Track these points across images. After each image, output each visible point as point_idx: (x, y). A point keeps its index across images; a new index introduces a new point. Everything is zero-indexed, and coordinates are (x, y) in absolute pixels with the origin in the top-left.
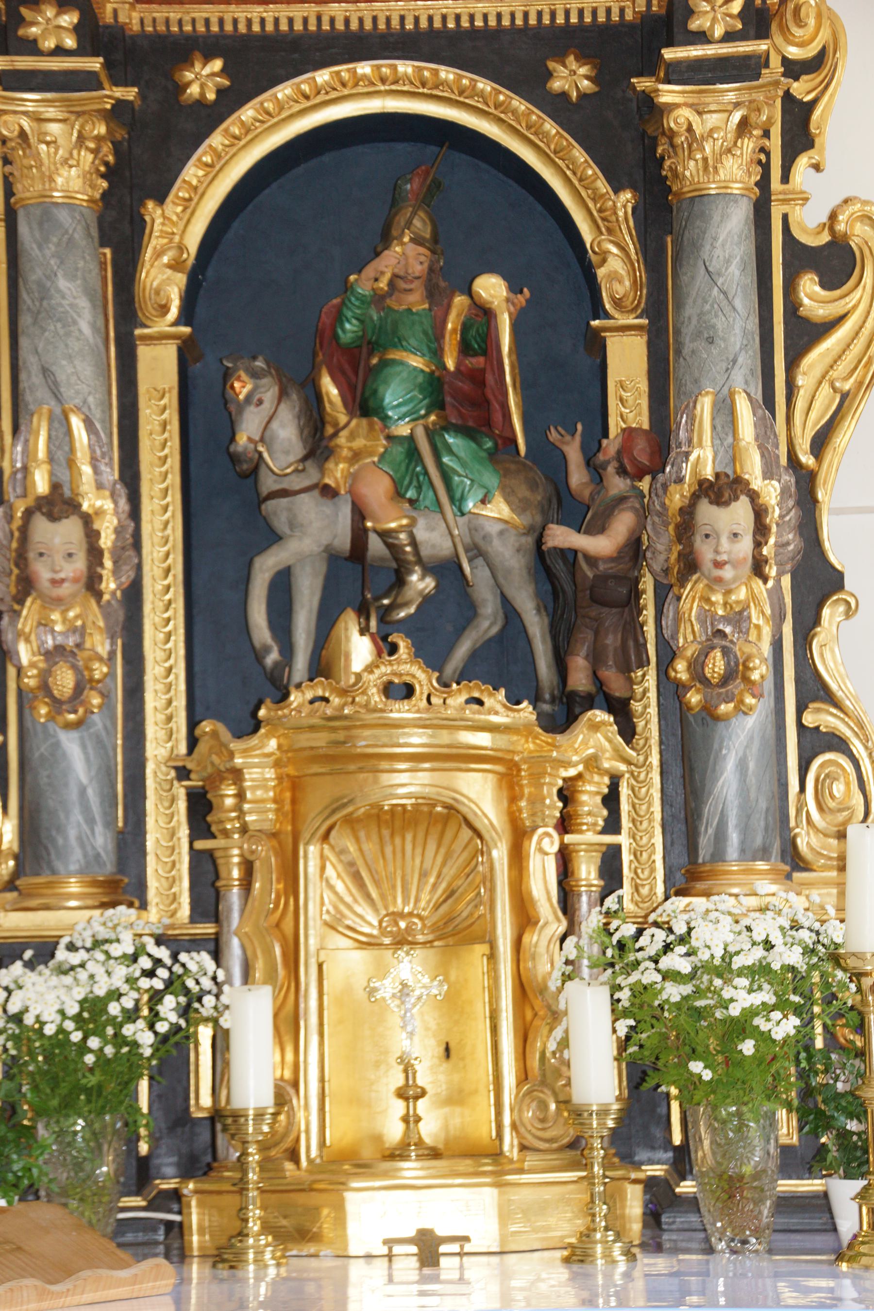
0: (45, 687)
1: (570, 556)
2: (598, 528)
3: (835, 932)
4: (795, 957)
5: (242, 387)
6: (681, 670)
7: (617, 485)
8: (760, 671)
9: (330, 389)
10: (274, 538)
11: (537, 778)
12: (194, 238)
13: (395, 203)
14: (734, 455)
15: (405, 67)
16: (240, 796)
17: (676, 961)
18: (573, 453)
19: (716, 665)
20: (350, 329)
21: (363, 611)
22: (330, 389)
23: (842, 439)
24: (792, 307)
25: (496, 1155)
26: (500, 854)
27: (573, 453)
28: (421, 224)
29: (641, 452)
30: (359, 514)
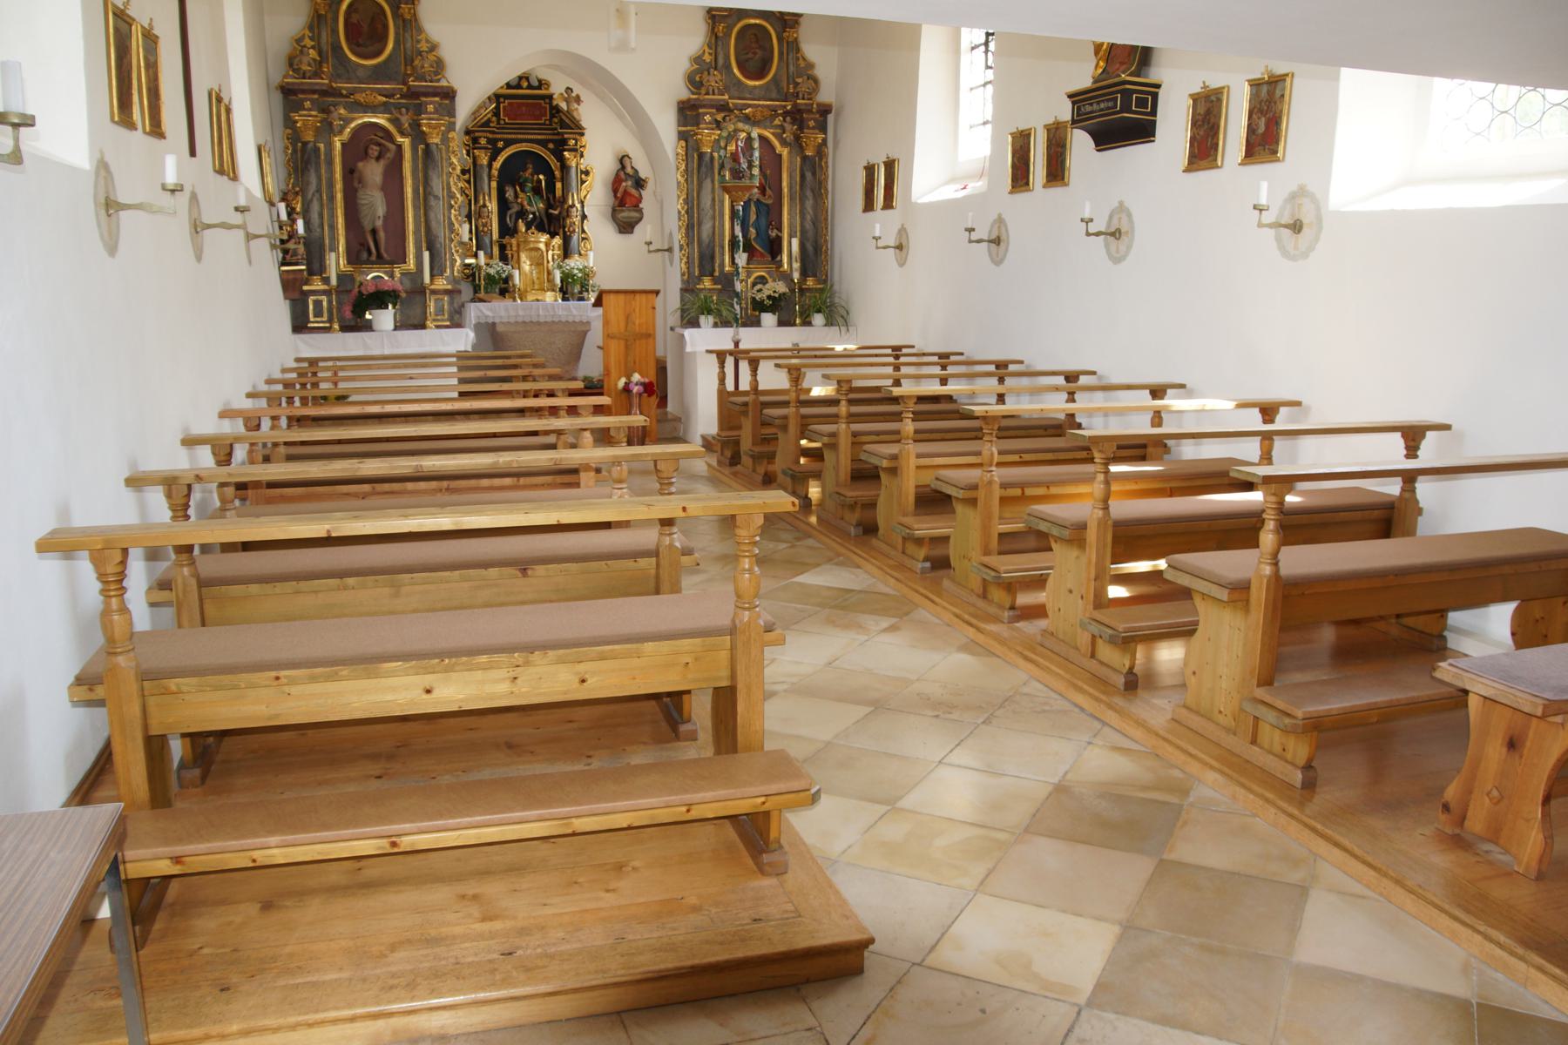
0: (483, 231)
1: (551, 214)
2: (555, 210)
3: (586, 264)
4: (581, 267)
5: (507, 188)
6: (566, 229)
7: (558, 204)
8: (577, 230)
9: (517, 187)
10: (509, 209)
11: (550, 244)
12: (498, 166)
13: (526, 164)
14: (573, 201)
15: (529, 144)
16: (511, 246)
17: (568, 267)
18: (551, 198)
19: (571, 229)
20: (521, 181)
21: (522, 219)
22: (517, 187)
23: (588, 197)
24: (581, 179)
25: (544, 290)
26: (545, 254)
27: (551, 198)
28: (531, 166)
29: (561, 200)
30: (522, 206)
